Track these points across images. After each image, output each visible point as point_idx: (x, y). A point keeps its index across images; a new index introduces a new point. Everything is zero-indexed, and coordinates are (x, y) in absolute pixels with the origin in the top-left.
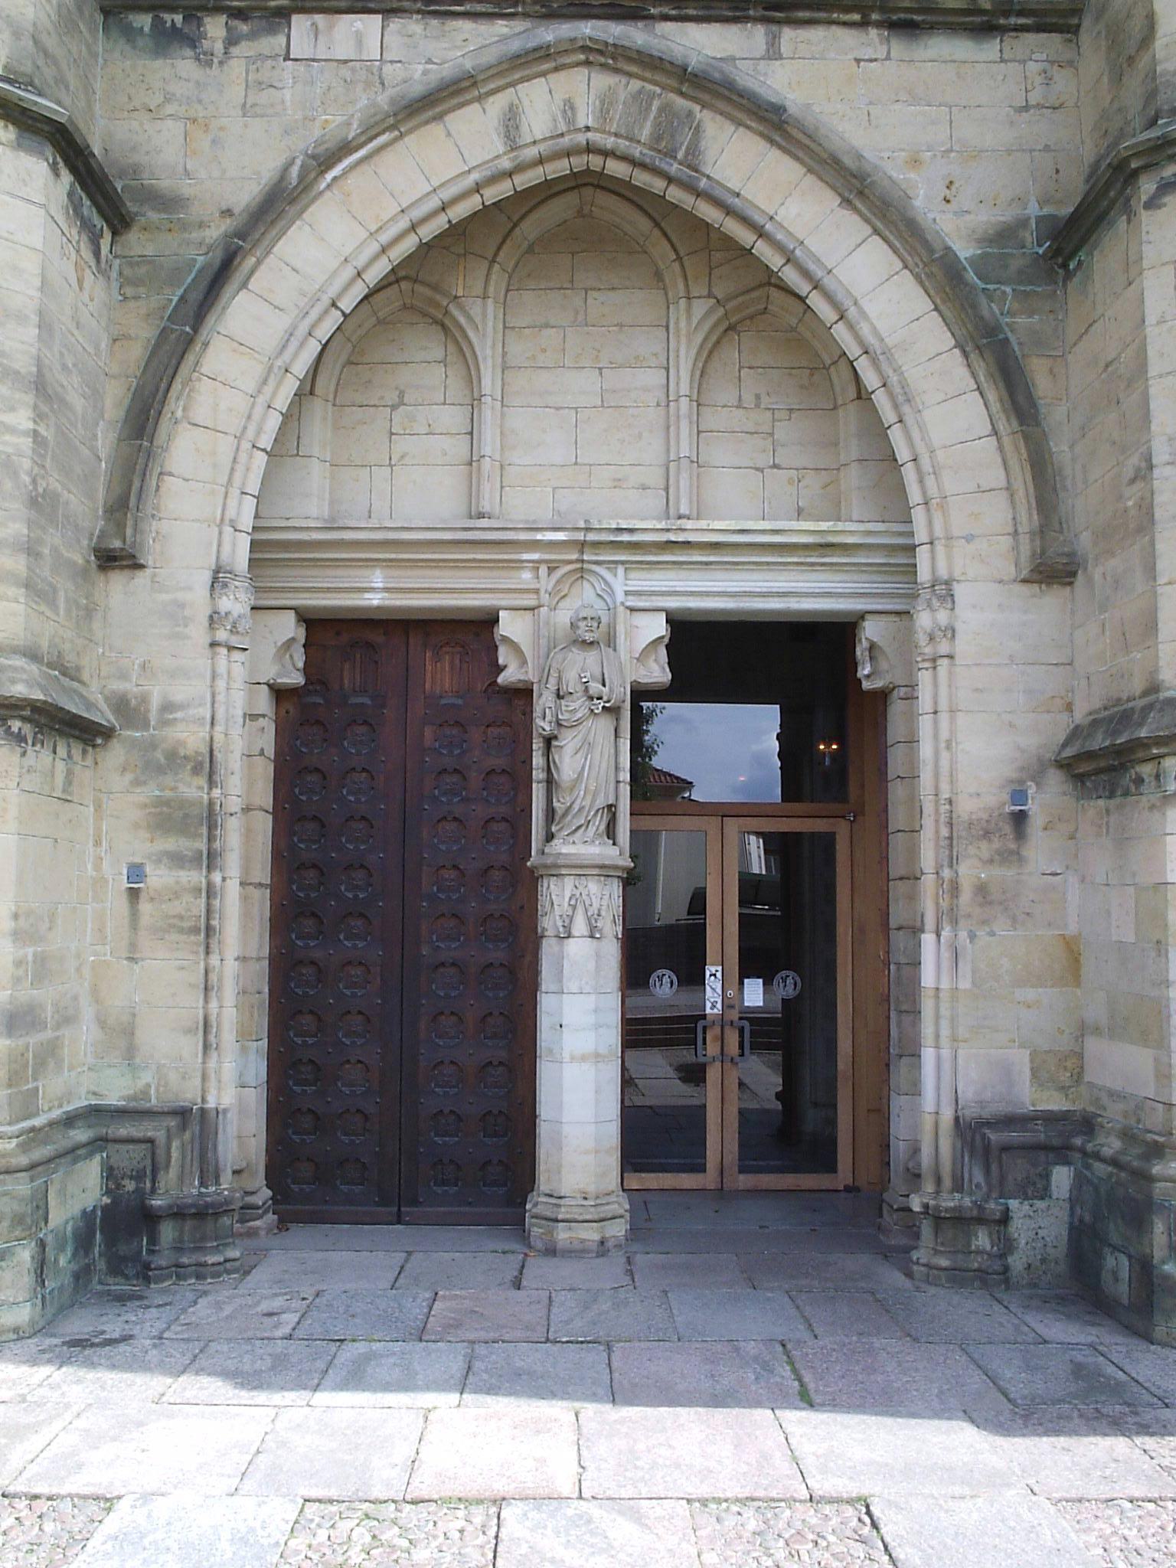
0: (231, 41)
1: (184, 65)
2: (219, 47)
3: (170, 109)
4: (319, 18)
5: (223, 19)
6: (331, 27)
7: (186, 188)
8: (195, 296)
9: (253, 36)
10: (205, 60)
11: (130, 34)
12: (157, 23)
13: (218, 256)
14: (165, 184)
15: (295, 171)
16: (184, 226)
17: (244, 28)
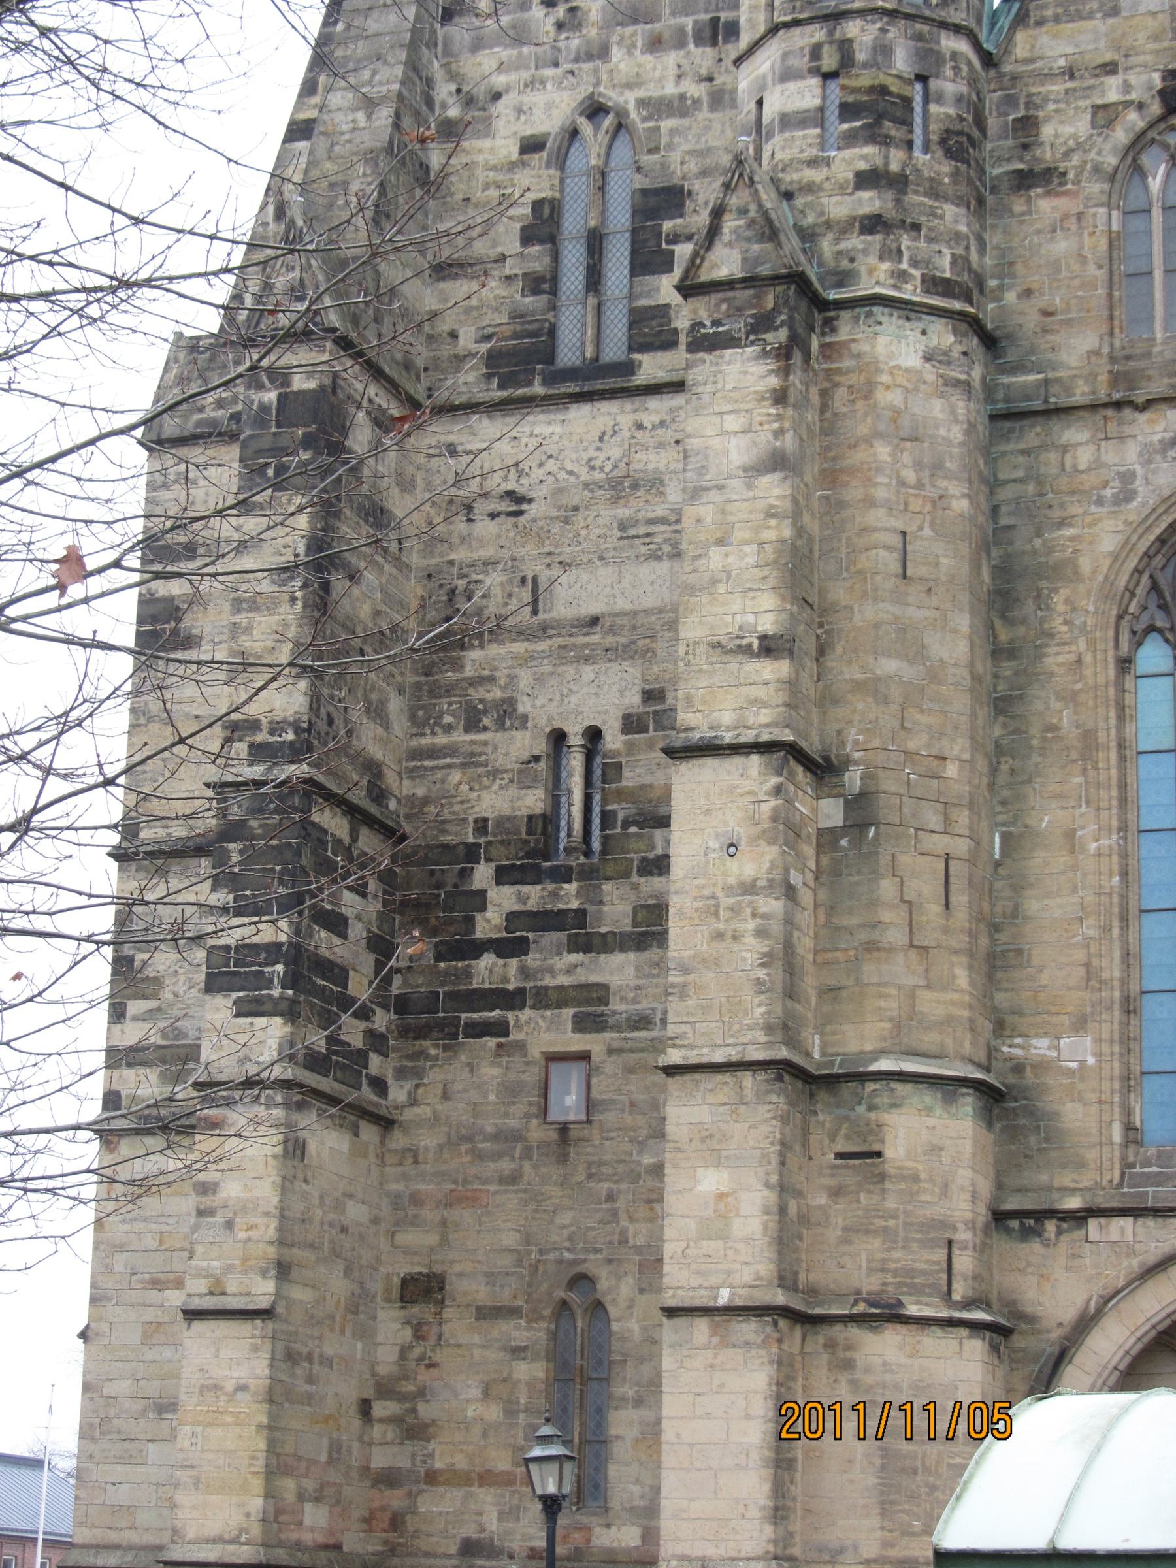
0: (1060, 1232)
1: (1036, 1246)
2: (1053, 1236)
3: (1030, 1270)
4: (1103, 1220)
5: (1054, 1221)
6: (1108, 1225)
7: (1039, 1311)
8: (1047, 1370)
9: (1068, 1231)
10: (1046, 1244)
11: (1008, 1231)
12: (1022, 1224)
13: (1056, 1350)
14: (1029, 1309)
15: (1093, 1304)
16: (1040, 1332)
17: (1065, 1225)
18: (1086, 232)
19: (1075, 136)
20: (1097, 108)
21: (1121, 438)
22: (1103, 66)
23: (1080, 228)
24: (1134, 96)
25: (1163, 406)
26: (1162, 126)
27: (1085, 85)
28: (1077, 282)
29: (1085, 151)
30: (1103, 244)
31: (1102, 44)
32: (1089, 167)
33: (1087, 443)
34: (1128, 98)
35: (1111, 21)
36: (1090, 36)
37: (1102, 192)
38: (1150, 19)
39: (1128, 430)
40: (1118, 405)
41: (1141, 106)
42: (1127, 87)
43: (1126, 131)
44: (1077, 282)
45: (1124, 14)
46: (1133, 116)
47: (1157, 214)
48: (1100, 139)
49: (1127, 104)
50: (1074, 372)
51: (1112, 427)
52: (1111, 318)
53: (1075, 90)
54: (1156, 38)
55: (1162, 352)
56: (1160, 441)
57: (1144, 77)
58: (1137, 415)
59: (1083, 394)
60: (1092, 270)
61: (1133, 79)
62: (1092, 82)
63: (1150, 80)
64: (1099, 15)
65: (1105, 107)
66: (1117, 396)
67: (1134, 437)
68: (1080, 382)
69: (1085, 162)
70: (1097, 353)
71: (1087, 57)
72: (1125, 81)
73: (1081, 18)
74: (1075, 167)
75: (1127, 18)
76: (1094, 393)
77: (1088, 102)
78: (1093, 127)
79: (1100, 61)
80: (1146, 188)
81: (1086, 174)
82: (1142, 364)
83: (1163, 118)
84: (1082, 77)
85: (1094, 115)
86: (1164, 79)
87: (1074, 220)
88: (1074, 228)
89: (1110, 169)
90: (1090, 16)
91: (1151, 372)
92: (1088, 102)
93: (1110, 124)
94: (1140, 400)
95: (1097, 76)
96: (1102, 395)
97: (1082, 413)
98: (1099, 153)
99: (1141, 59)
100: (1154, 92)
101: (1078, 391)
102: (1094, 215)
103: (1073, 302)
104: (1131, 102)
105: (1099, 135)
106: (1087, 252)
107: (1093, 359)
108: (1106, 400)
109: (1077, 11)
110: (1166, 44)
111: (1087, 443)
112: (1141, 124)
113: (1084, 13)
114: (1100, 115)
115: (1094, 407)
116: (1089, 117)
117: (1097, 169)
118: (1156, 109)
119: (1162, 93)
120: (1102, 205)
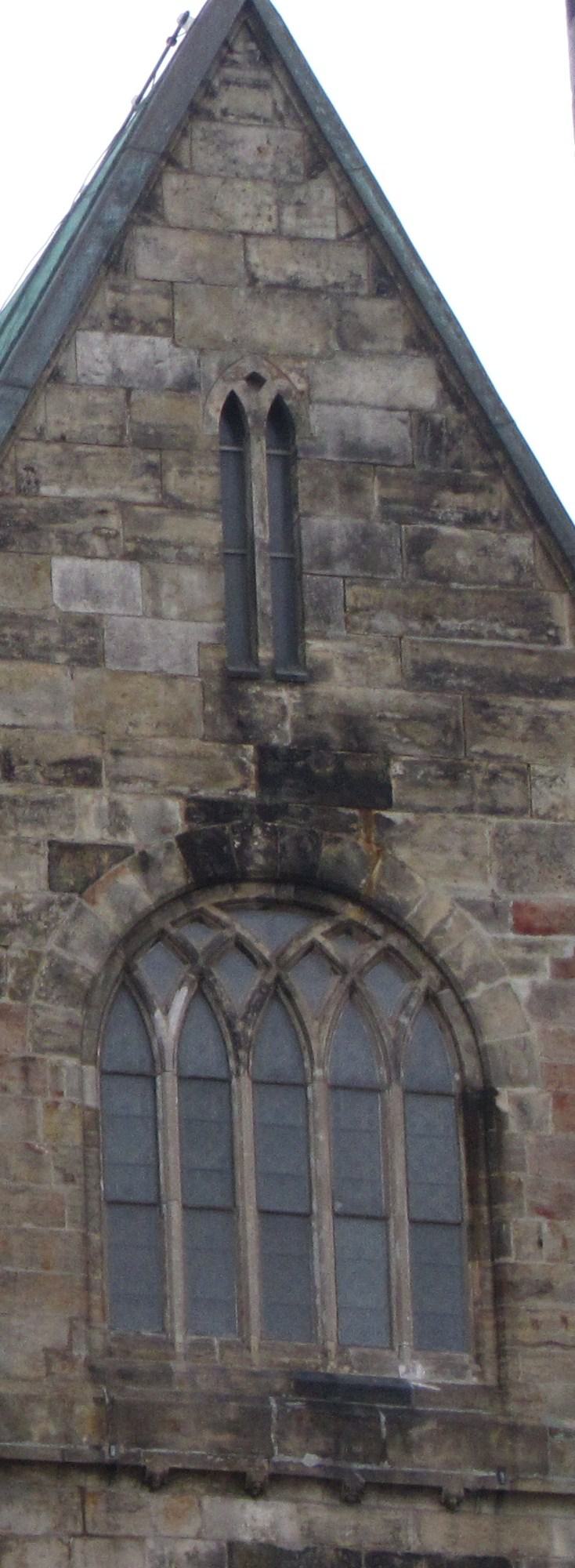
18: (40, 1107)
19: (16, 899)
20: (60, 851)
21: (114, 1540)
22: (71, 763)
23: (28, 1090)
24: (131, 839)
25: (199, 1488)
26: (181, 910)
27: (35, 795)
28: (22, 1201)
29: (36, 933)
30: (74, 1128)
31: (68, 719)
32: (44, 965)
33: (47, 1537)
34: (120, 840)
35: (84, 675)
36: (46, 698)
37: (69, 1023)
38: (161, 686)
39: (127, 1524)
40: (110, 1471)
41: (145, 863)
42: (117, 818)
43: (117, 907)
44: (22, 1201)
45: (110, 665)
46: (130, 880)
47: (168, 1085)
48: (66, 915)
49: (120, 853)
50: (22, 1389)
51: (95, 1511)
52: (88, 1287)
53: (14, 801)
54: (176, 728)
55: (192, 1374)
56: (191, 1557)
57: (151, 804)
58: (145, 1495)
59: (45, 1438)
60: (52, 1180)
61: (129, 803)
62: (50, 792)
63: (163, 812)
64: (61, 658)
65: (76, 849)
66: (113, 1452)
67: (140, 1540)
68: (41, 1412)
69: (38, 956)
70: (64, 1355)
71: (40, 739)
72: (114, 805)
73: (27, 656)
74: (15, 961)
75: (116, 675)
76: (67, 1437)
77: (42, 833)
78: (52, 887)
79: (64, 753)
80: (147, 1032)
81: (38, 982)
82: (156, 1393)
83: (184, 895)
84: (29, 779)
85: (53, 861)
86: (188, 815)
87: (15, 1071)
88: (16, 1087)
89: (85, 979)
90: (43, 655)
91: (179, 1414)
92: (42, 833)
93: (85, 886)
94: (159, 1468)
95: (58, 782)
96: (84, 1443)
97: (37, 1475)
98: (64, 942)
99: (148, 765)
100: (171, 839)
101: (36, 1431)
102: (55, 1070)
103: (16, 1241)
104: (127, 851)
105: (65, 904)
106: (40, 1143)
107: (57, 1367)
108: (92, 1457)
109: (17, 638)
110: (194, 744)
111: (47, 1537)
112: (146, 900)
113: (32, 648)
114: (65, 863)
115: (63, 1467)
116: (44, 863)
117: (60, 975)
118: (174, 873)
119: (185, 842)
120: (72, 1051)
